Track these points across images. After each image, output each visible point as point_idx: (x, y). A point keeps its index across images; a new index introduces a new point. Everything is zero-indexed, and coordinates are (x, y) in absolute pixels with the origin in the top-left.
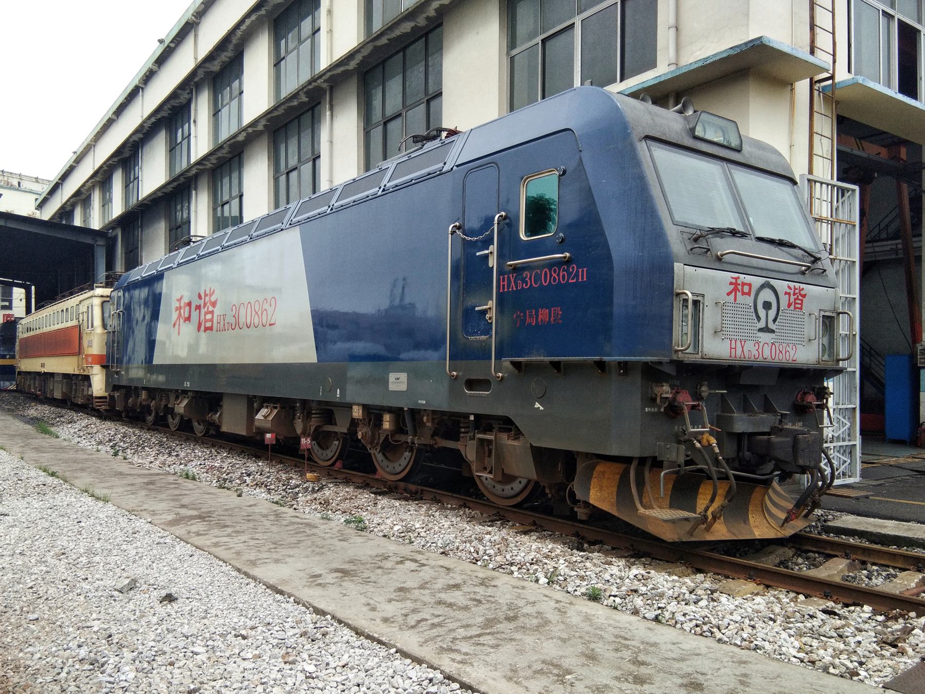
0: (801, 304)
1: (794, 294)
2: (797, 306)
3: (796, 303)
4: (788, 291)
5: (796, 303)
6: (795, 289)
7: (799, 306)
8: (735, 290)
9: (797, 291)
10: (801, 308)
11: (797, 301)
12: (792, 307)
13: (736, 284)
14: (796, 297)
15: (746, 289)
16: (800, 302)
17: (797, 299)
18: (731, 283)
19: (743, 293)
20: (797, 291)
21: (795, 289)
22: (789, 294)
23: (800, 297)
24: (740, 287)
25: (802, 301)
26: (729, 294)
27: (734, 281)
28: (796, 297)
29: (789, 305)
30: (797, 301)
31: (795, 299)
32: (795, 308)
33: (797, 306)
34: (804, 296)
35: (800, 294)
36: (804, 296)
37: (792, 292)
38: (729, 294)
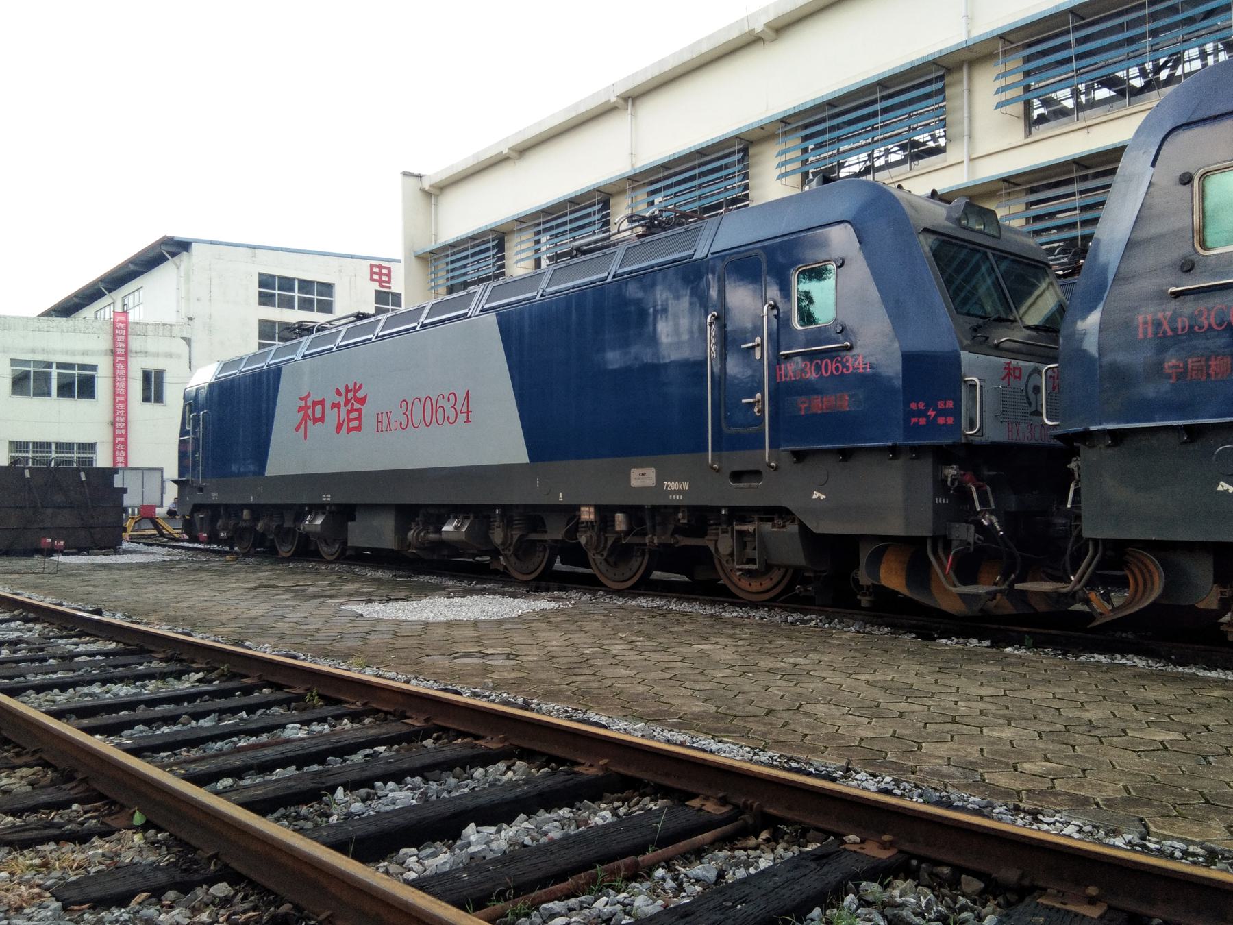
0: (359, 419)
1: (347, 402)
2: (353, 424)
3: (349, 420)
4: (337, 399)
5: (349, 420)
6: (348, 391)
8: (306, 416)
9: (351, 395)
10: (358, 429)
14: (349, 407)
17: (353, 410)
18: (300, 409)
19: (316, 420)
23: (357, 406)
24: (310, 411)
25: (360, 411)
26: (297, 429)
27: (302, 404)
28: (349, 407)
31: (349, 412)
32: (349, 430)
36: (362, 401)
37: (342, 400)
38: (297, 429)
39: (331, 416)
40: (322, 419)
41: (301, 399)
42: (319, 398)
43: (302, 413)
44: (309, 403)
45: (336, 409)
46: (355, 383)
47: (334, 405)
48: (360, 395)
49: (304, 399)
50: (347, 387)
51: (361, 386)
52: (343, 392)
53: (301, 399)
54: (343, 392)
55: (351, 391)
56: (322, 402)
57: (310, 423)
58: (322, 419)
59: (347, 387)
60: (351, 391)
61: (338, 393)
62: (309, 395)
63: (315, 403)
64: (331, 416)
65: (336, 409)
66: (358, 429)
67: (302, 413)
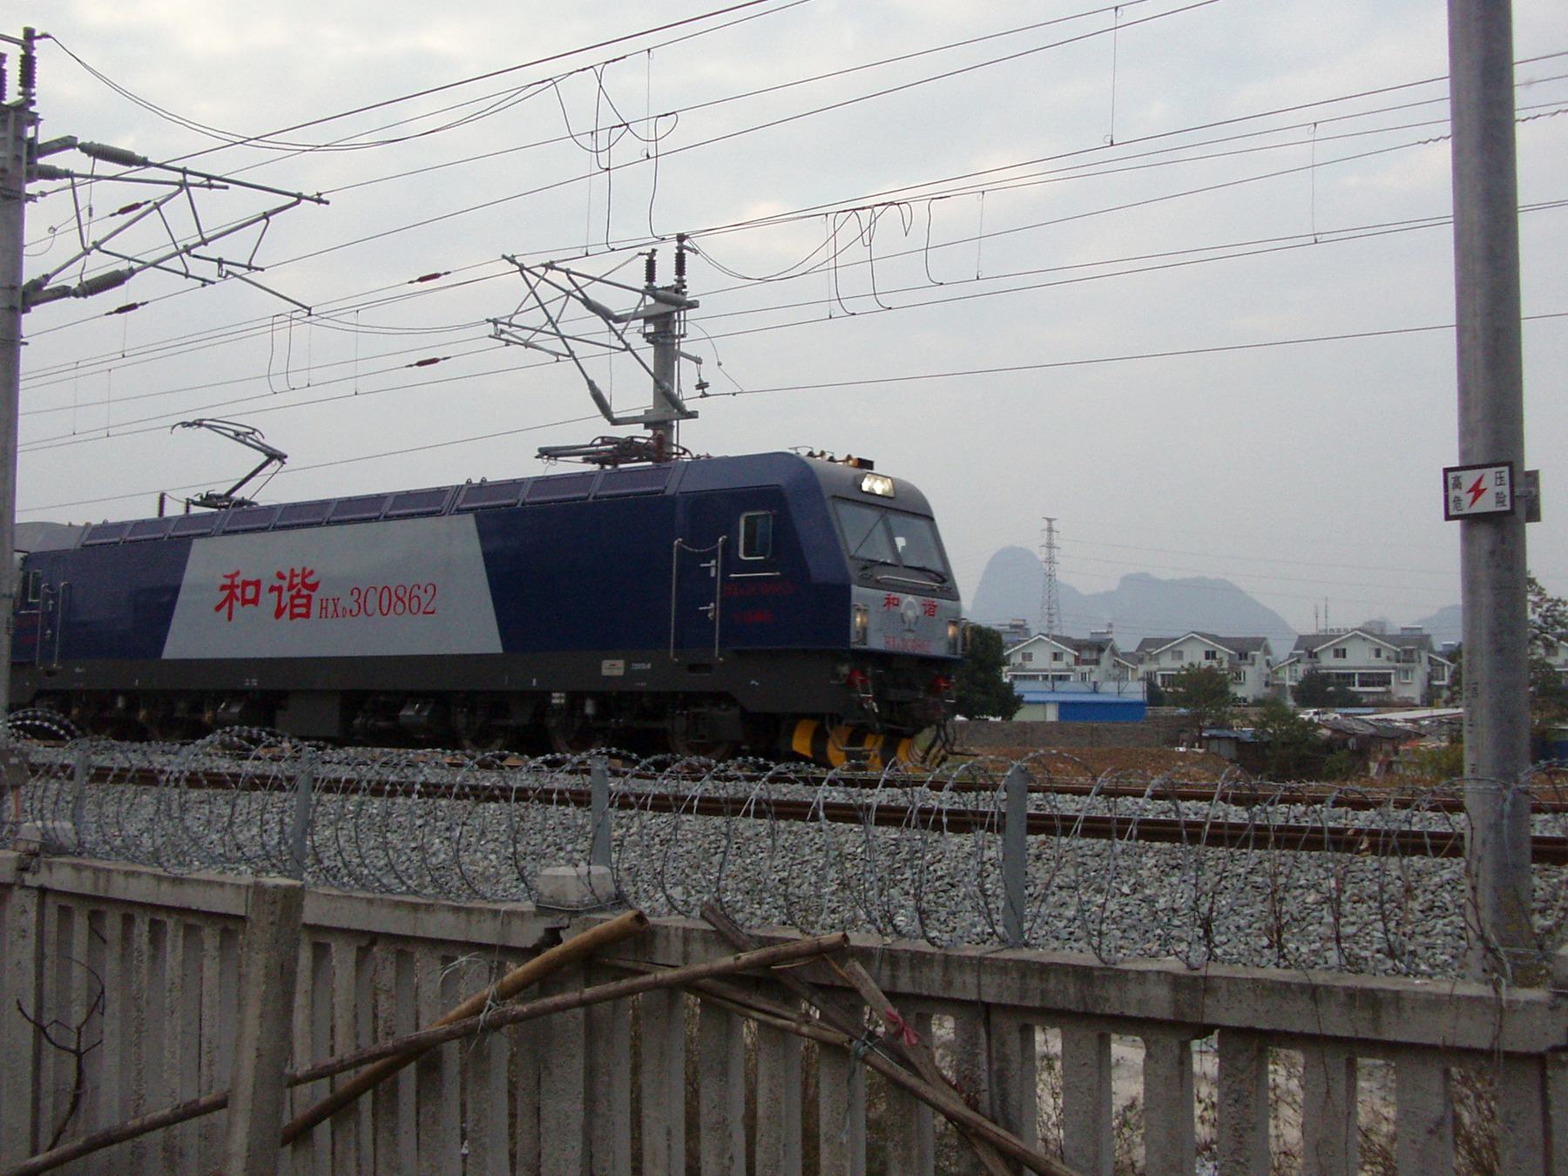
0: (308, 605)
1: (291, 587)
2: (303, 610)
4: (277, 583)
5: (293, 606)
6: (293, 574)
7: (303, 610)
8: (231, 598)
9: (297, 580)
10: (307, 615)
11: (297, 601)
12: (288, 611)
13: (232, 587)
14: (294, 592)
15: (250, 592)
16: (304, 601)
17: (299, 595)
18: (223, 588)
19: (245, 602)
20: (297, 580)
21: (293, 574)
22: (280, 589)
23: (305, 592)
24: (238, 592)
25: (309, 597)
26: (218, 608)
27: (228, 582)
28: (294, 592)
29: (279, 613)
30: (297, 601)
31: (293, 598)
32: (293, 616)
33: (297, 610)
34: (314, 587)
35: (305, 585)
36: (314, 587)
37: (285, 584)
38: (218, 608)
39: (269, 601)
40: (255, 601)
41: (226, 576)
42: (253, 578)
43: (226, 593)
44: (238, 581)
45: (276, 594)
46: (304, 569)
47: (272, 589)
48: (310, 581)
49: (232, 577)
50: (293, 570)
51: (311, 573)
52: (287, 574)
53: (226, 576)
54: (287, 574)
55: (297, 576)
56: (257, 584)
57: (237, 604)
58: (255, 601)
59: (293, 570)
60: (297, 576)
61: (281, 576)
62: (238, 573)
63: (246, 584)
64: (269, 601)
65: (276, 594)
66: (307, 615)
67: (226, 593)
